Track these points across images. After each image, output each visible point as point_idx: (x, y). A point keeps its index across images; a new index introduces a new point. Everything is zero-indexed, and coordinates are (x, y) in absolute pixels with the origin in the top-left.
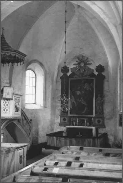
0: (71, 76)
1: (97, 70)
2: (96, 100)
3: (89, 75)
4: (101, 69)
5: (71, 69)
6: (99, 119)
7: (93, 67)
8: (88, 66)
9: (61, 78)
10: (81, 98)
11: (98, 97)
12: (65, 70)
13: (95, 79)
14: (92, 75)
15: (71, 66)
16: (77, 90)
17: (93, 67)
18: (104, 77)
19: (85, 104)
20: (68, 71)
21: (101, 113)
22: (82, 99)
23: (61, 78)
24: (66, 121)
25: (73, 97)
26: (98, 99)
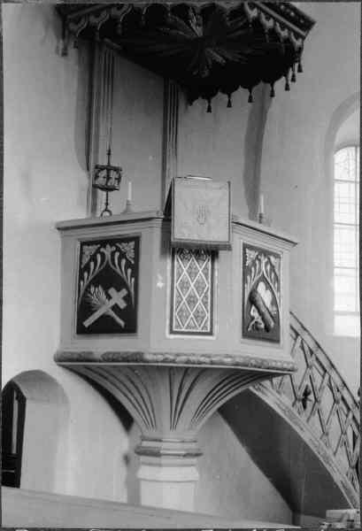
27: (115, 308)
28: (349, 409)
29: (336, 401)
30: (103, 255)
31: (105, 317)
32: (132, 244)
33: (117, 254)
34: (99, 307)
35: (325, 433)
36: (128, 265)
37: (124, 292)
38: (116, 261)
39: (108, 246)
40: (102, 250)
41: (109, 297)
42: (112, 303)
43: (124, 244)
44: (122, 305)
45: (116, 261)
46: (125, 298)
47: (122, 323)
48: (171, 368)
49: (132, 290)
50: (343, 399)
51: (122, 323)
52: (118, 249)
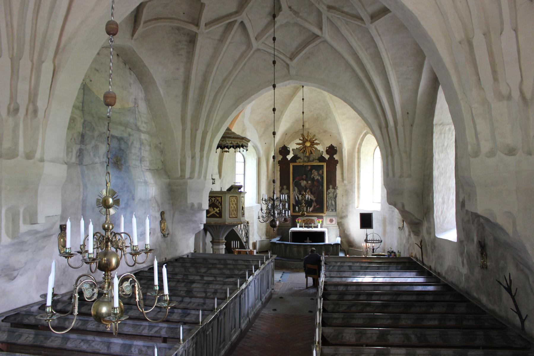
0: (295, 158)
1: (328, 152)
2: (328, 193)
3: (317, 158)
4: (332, 150)
5: (293, 150)
6: (331, 218)
7: (321, 148)
8: (316, 146)
9: (279, 162)
10: (307, 191)
11: (329, 188)
12: (284, 151)
13: (325, 165)
14: (321, 159)
15: (293, 146)
16: (303, 180)
17: (321, 148)
18: (337, 162)
19: (314, 199)
20: (288, 153)
21: (334, 210)
22: (308, 192)
23: (279, 162)
24: (288, 222)
25: (296, 188)
26: (329, 191)
27: (216, 212)
28: (246, 227)
29: (244, 226)
30: (212, 200)
31: (213, 214)
32: (220, 198)
33: (216, 200)
34: (211, 212)
35: (242, 234)
36: (219, 203)
37: (218, 209)
38: (216, 202)
39: (213, 198)
40: (212, 199)
41: (214, 210)
42: (215, 211)
43: (218, 198)
44: (218, 212)
45: (216, 202)
46: (219, 210)
47: (218, 216)
48: (231, 225)
49: (221, 209)
50: (245, 225)
51: (218, 216)
52: (216, 199)
